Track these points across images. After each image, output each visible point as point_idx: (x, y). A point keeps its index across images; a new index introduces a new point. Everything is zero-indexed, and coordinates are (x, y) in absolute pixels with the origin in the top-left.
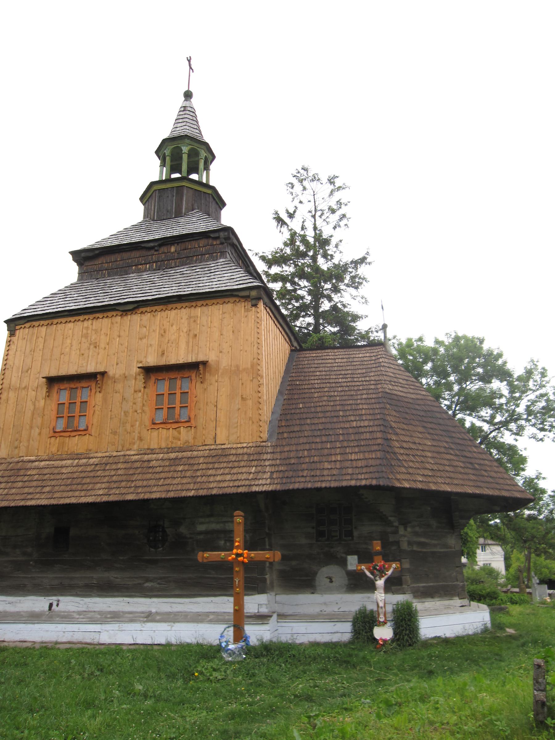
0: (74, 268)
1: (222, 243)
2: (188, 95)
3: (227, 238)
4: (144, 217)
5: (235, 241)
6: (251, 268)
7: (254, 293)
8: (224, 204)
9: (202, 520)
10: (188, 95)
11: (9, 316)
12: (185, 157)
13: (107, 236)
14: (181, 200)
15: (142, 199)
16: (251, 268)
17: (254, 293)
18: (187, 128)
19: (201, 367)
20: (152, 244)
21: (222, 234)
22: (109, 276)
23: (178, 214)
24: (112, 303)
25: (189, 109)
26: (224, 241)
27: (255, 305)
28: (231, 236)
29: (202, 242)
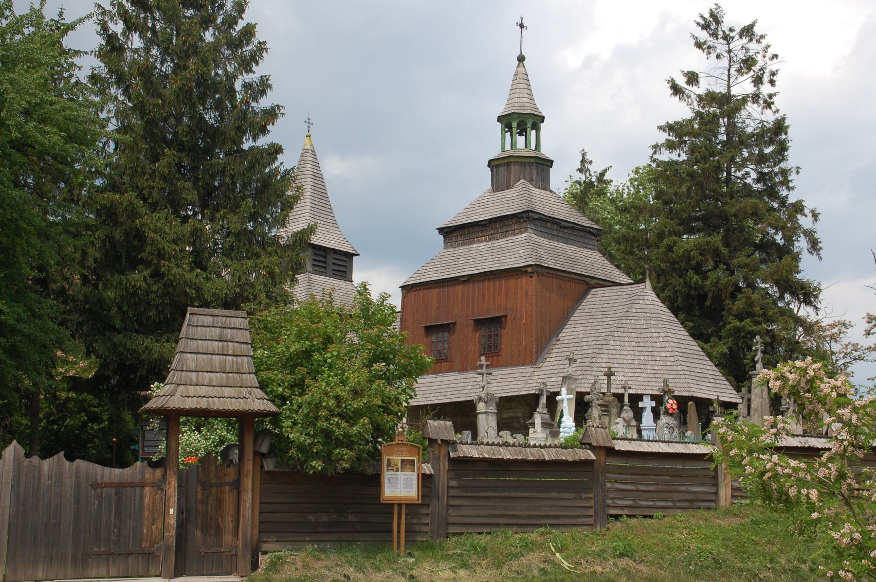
0: (442, 237)
1: (526, 221)
2: (521, 59)
3: (528, 218)
4: (492, 185)
5: (536, 216)
6: (563, 223)
7: (529, 270)
8: (552, 162)
9: (506, 411)
10: (521, 59)
11: (401, 284)
12: (514, 130)
13: (461, 210)
14: (510, 174)
15: (489, 166)
16: (563, 223)
17: (529, 270)
18: (515, 100)
19: (503, 319)
20: (484, 223)
21: (525, 215)
22: (462, 245)
23: (508, 187)
24: (456, 275)
25: (520, 76)
26: (526, 219)
27: (531, 277)
28: (531, 214)
29: (514, 221)
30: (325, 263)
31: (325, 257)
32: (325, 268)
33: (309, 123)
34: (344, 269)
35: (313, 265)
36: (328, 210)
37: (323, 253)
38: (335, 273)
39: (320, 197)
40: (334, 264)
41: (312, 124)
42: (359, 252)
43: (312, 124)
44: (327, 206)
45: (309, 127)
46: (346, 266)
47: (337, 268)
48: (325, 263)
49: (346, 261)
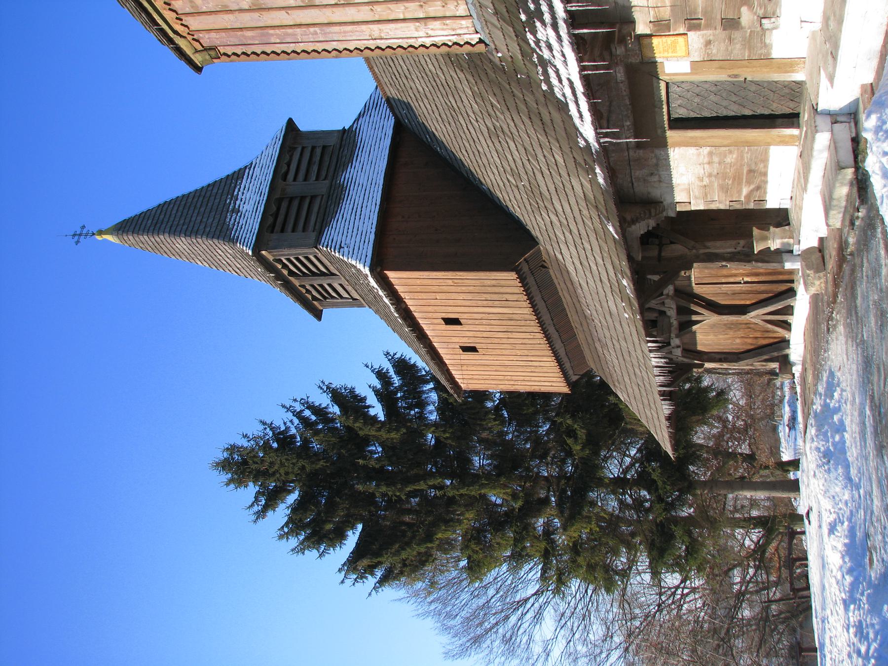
30: (303, 198)
31: (291, 199)
32: (313, 198)
33: (80, 235)
34: (318, 151)
35: (304, 230)
36: (215, 191)
37: (284, 205)
38: (323, 177)
39: (192, 208)
40: (305, 179)
41: (84, 227)
42: (283, 123)
43: (84, 227)
44: (208, 194)
45: (86, 235)
46: (313, 148)
47: (315, 168)
48: (303, 198)
49: (303, 148)
